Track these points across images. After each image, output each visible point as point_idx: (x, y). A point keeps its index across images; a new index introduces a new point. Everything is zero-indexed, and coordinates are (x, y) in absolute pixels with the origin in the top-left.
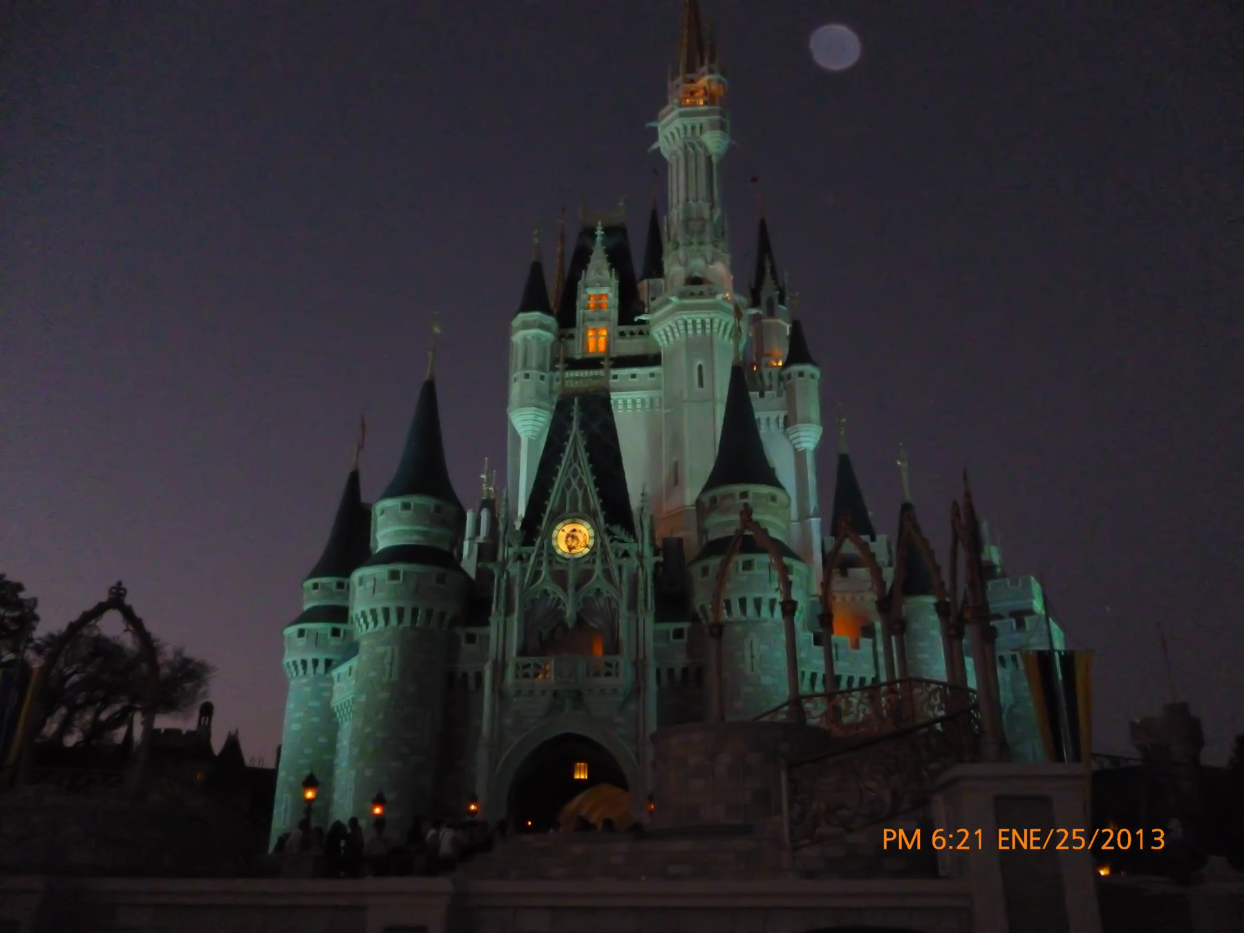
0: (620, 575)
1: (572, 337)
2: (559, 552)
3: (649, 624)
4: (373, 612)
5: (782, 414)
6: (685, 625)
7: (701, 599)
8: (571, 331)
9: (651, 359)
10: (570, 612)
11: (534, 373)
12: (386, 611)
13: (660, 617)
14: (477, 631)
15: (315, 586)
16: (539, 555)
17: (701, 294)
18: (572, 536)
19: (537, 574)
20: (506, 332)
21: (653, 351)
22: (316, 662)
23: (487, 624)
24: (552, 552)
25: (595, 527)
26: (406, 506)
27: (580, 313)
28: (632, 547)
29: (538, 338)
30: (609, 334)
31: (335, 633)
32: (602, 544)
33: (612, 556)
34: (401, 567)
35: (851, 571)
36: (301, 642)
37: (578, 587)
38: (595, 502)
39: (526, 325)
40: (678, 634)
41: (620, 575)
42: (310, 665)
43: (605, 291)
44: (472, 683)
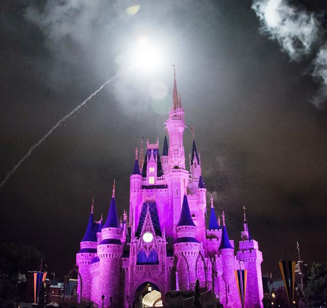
1: (145, 179)
2: (145, 240)
3: (165, 257)
4: (104, 254)
6: (173, 257)
7: (176, 252)
8: (145, 178)
10: (147, 254)
11: (137, 190)
12: (107, 255)
13: (167, 256)
14: (126, 258)
15: (85, 243)
19: (140, 246)
20: (130, 179)
21: (165, 184)
22: (86, 262)
23: (129, 257)
25: (154, 235)
26: (110, 230)
27: (147, 173)
28: (161, 239)
31: (90, 255)
34: (110, 245)
35: (212, 239)
36: (82, 257)
37: (149, 249)
38: (153, 229)
39: (135, 178)
40: (171, 259)
42: (84, 263)
44: (126, 270)
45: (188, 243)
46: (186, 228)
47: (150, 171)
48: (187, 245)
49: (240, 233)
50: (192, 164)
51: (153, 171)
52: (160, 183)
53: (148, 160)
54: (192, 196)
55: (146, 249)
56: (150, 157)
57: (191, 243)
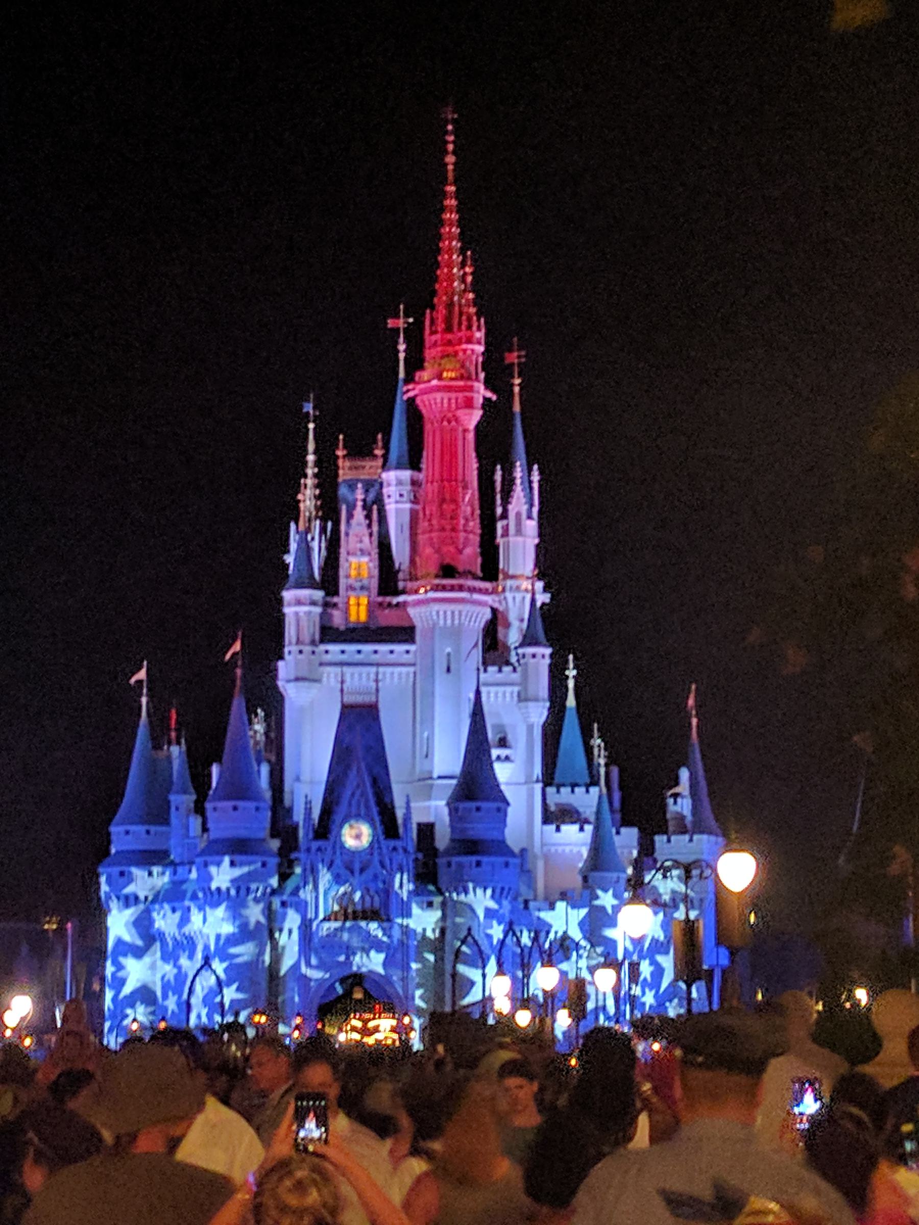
0: (391, 864)
5: (516, 689)
8: (335, 599)
9: (406, 634)
11: (307, 649)
16: (334, 847)
17: (452, 588)
18: (358, 837)
24: (342, 846)
27: (343, 583)
29: (310, 613)
30: (369, 602)
32: (378, 840)
33: (385, 851)
35: (564, 828)
37: (362, 870)
39: (299, 602)
41: (391, 864)
43: (365, 559)
45: (485, 859)
46: (478, 809)
47: (353, 573)
48: (478, 864)
49: (663, 807)
50: (505, 516)
51: (365, 574)
52: (387, 618)
53: (343, 527)
54: (500, 671)
55: (352, 872)
56: (350, 516)
57: (492, 859)
